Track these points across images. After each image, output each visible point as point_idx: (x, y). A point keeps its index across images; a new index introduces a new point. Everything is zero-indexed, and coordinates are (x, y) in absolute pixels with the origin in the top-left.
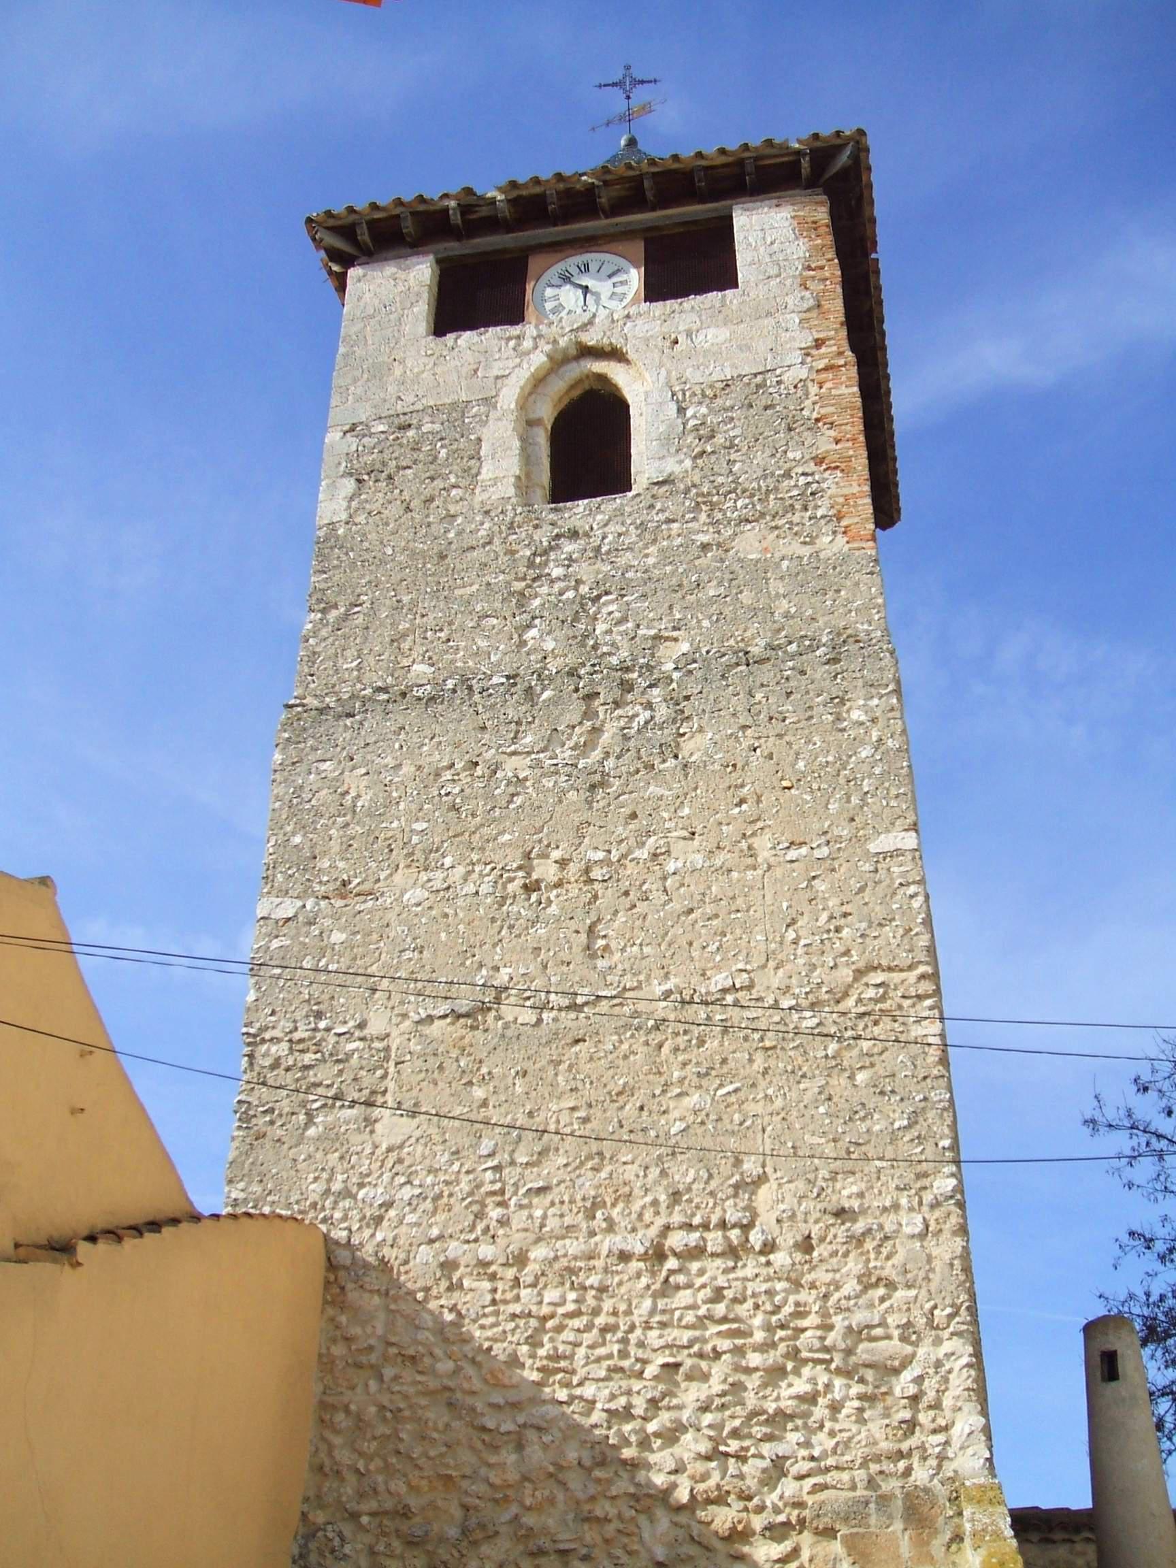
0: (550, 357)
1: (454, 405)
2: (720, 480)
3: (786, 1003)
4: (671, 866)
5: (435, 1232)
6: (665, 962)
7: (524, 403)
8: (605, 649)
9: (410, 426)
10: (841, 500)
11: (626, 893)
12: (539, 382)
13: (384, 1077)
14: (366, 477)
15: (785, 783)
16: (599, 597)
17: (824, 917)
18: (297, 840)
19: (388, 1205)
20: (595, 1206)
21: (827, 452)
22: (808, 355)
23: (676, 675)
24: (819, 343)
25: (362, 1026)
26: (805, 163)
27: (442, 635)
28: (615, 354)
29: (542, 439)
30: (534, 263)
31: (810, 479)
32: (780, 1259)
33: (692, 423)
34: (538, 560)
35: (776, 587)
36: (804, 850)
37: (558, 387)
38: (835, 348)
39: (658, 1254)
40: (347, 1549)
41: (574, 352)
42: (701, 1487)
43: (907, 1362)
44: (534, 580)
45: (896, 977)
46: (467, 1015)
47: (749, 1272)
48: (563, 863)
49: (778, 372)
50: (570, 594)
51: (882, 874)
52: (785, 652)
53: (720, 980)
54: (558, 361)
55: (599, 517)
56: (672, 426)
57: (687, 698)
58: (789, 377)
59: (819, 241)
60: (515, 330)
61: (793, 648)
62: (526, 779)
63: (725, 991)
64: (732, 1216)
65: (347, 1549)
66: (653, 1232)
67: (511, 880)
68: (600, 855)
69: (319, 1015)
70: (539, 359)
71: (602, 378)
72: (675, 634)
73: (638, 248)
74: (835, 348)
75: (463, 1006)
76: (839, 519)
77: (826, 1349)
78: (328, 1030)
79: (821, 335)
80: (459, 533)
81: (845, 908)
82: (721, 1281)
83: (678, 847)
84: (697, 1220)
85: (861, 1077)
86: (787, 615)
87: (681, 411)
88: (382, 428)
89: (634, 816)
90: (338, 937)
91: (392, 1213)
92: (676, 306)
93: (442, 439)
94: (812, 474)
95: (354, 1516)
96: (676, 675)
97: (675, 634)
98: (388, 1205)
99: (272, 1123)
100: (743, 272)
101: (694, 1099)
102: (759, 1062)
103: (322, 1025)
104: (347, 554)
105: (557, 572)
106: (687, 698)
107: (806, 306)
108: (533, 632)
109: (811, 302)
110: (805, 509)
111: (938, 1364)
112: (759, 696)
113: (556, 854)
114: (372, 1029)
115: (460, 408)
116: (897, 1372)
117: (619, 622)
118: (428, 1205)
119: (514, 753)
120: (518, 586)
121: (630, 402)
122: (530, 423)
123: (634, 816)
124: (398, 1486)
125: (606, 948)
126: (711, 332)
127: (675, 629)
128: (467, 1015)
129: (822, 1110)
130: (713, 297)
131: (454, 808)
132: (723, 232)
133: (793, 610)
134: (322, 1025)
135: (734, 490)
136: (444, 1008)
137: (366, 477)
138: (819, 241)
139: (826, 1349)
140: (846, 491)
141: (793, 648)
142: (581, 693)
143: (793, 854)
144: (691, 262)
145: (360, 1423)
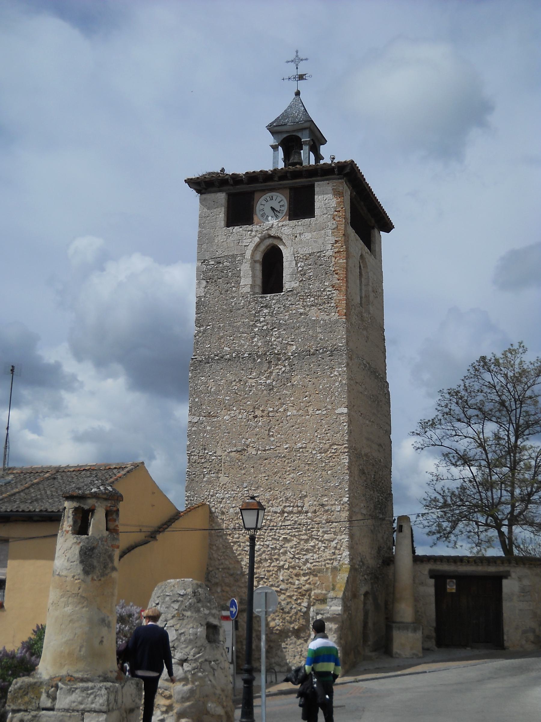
0: (260, 239)
1: (233, 255)
2: (306, 291)
3: (314, 452)
4: (289, 413)
5: (234, 505)
6: (287, 440)
7: (253, 255)
8: (274, 346)
10: (338, 301)
11: (278, 420)
12: (258, 246)
13: (221, 466)
15: (317, 392)
16: (273, 329)
17: (324, 430)
18: (197, 400)
19: (223, 499)
20: (270, 501)
22: (333, 246)
23: (292, 357)
24: (336, 242)
25: (215, 453)
28: (279, 238)
29: (259, 267)
30: (256, 195)
31: (330, 293)
32: (309, 514)
33: (300, 269)
35: (319, 330)
36: (320, 412)
37: (263, 247)
39: (283, 512)
40: (217, 576)
42: (290, 565)
43: (334, 539)
44: (256, 322)
45: (340, 447)
46: (240, 451)
47: (303, 517)
48: (263, 411)
50: (265, 328)
51: (338, 419)
53: (299, 445)
54: (262, 240)
55: (273, 301)
56: (294, 270)
57: (294, 365)
60: (250, 227)
62: (254, 386)
63: (300, 448)
64: (299, 504)
65: (217, 576)
66: (282, 507)
67: (250, 415)
68: (272, 409)
69: (205, 449)
70: (257, 240)
72: (292, 343)
73: (288, 192)
75: (239, 448)
76: (337, 308)
77: (318, 536)
78: (207, 453)
80: (235, 304)
81: (329, 428)
82: (296, 519)
83: (290, 408)
84: (292, 505)
85: (329, 472)
86: (321, 339)
87: (296, 264)
88: (213, 263)
89: (280, 399)
90: (208, 428)
91: (224, 500)
92: (297, 223)
94: (331, 291)
95: (218, 569)
96: (292, 357)
97: (292, 343)
98: (223, 499)
99: (195, 477)
100: (317, 212)
101: (291, 476)
102: (307, 467)
103: (206, 452)
105: (262, 319)
106: (294, 365)
108: (256, 339)
109: (335, 226)
110: (328, 303)
111: (341, 540)
112: (312, 365)
113: (261, 409)
114: (218, 453)
115: (234, 256)
116: (332, 541)
117: (278, 338)
118: (232, 499)
119: (250, 378)
122: (255, 262)
123: (280, 399)
124: (227, 562)
125: (272, 435)
126: (306, 234)
127: (292, 341)
128: (240, 451)
129: (320, 480)
130: (307, 220)
131: (236, 393)
132: (313, 186)
134: (206, 452)
135: (310, 295)
136: (235, 449)
139: (318, 536)
140: (340, 298)
142: (267, 361)
143: (318, 412)
144: (301, 207)
145: (218, 549)
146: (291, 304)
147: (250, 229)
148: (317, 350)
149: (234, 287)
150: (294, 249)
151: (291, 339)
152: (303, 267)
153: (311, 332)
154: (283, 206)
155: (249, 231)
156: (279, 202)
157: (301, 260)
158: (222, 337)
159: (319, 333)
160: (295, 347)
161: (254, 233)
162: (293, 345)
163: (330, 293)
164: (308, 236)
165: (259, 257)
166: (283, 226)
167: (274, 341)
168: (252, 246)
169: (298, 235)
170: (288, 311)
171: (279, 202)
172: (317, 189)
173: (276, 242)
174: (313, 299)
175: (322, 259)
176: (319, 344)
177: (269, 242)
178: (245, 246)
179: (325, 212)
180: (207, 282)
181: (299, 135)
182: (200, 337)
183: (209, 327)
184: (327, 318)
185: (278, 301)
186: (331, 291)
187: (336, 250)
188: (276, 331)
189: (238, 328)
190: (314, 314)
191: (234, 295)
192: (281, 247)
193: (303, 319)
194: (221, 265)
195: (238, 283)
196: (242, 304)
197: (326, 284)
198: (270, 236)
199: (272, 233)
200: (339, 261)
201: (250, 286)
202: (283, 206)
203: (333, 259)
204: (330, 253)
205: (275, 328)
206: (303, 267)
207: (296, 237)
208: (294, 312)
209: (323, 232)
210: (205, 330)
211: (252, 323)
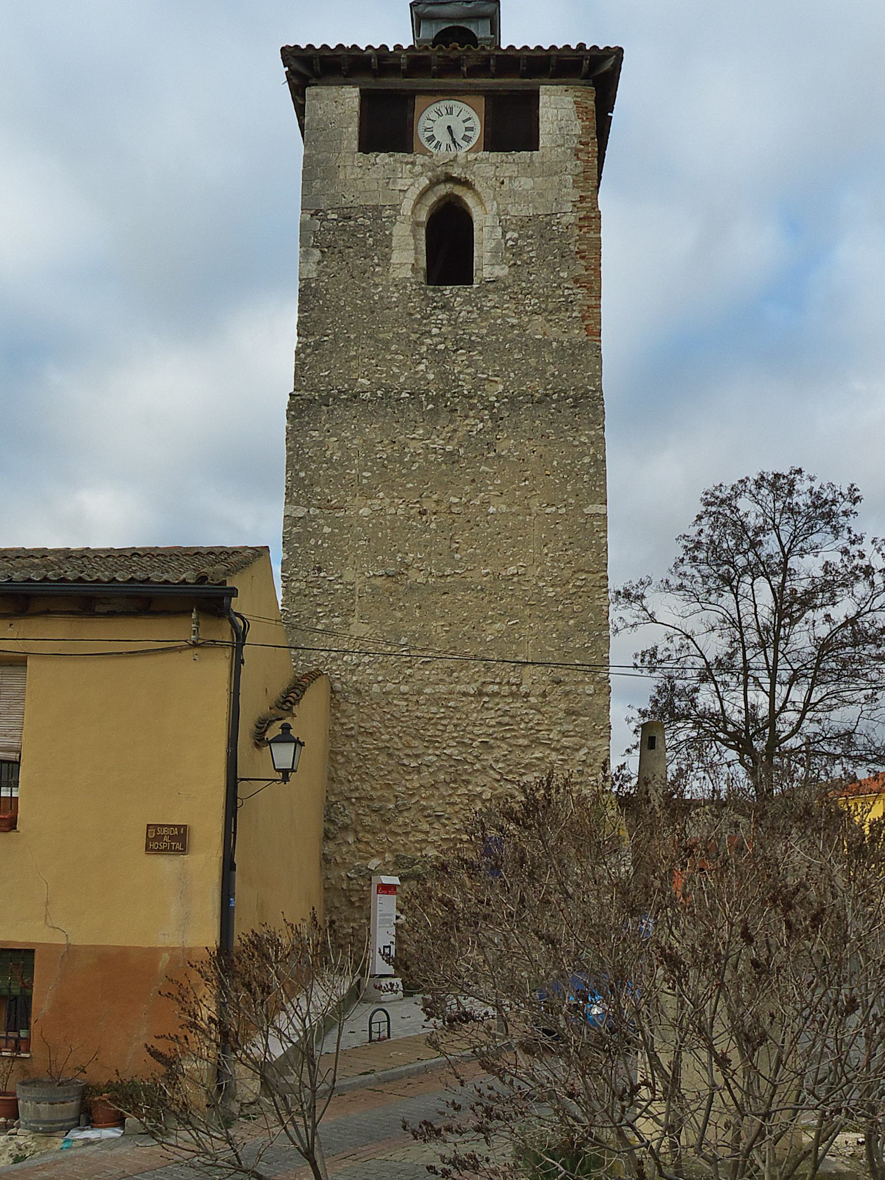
1: (375, 208)
2: (524, 284)
3: (541, 584)
4: (492, 510)
5: (380, 678)
6: (486, 558)
8: (460, 383)
9: (350, 217)
10: (586, 308)
11: (469, 521)
12: (423, 194)
13: (352, 603)
14: (326, 250)
15: (547, 472)
16: (457, 350)
17: (561, 544)
18: (302, 474)
19: (358, 665)
20: (453, 671)
21: (580, 275)
22: (575, 206)
23: (496, 405)
24: (582, 199)
25: (340, 577)
26: (586, 63)
27: (373, 361)
28: (466, 184)
30: (419, 101)
31: (571, 292)
32: (532, 700)
33: (510, 243)
34: (425, 321)
35: (548, 358)
36: (554, 509)
37: (432, 199)
38: (590, 205)
39: (480, 694)
40: (347, 812)
41: (443, 178)
42: (496, 792)
43: (582, 746)
44: (422, 334)
45: (591, 576)
46: (393, 576)
47: (519, 705)
48: (437, 502)
49: (559, 215)
50: (442, 347)
51: (588, 526)
52: (551, 398)
53: (512, 570)
54: (434, 183)
56: (499, 243)
57: (502, 419)
58: (564, 220)
59: (587, 123)
60: (409, 158)
61: (555, 396)
62: (420, 454)
63: (513, 575)
64: (513, 680)
65: (347, 812)
66: (478, 684)
67: (412, 508)
68: (457, 500)
69: (320, 570)
70: (424, 182)
71: (458, 198)
72: (496, 379)
73: (481, 101)
74: (590, 205)
75: (392, 570)
77: (549, 739)
78: (324, 577)
79: (583, 194)
80: (381, 298)
81: (570, 540)
82: (507, 708)
83: (494, 501)
84: (498, 680)
85: (571, 622)
86: (553, 375)
87: (504, 233)
88: (335, 216)
89: (473, 481)
90: (327, 530)
91: (360, 668)
92: (504, 158)
93: (370, 231)
95: (348, 799)
96: (496, 405)
97: (496, 379)
98: (358, 665)
99: (299, 622)
101: (497, 626)
102: (527, 612)
103: (322, 574)
104: (318, 301)
106: (502, 419)
107: (577, 172)
108: (422, 367)
109: (581, 169)
110: (567, 310)
111: (594, 748)
112: (538, 422)
113: (435, 497)
114: (345, 579)
115: (377, 209)
116: (577, 750)
118: (377, 665)
119: (414, 439)
120: (414, 337)
121: (475, 218)
122: (418, 224)
123: (473, 481)
124: (367, 786)
125: (457, 549)
128: (393, 576)
129: (554, 635)
131: (384, 466)
133: (557, 373)
134: (322, 574)
136: (381, 572)
137: (326, 250)
138: (587, 123)
139: (549, 739)
140: (588, 303)
141: (555, 396)
142: (447, 409)
143: (548, 510)
145: (349, 761)
146: (494, 307)
147: (410, 160)
148: (547, 395)
149: (378, 265)
150: (498, 204)
151: (494, 371)
152: (518, 239)
153: (533, 361)
154: (471, 129)
155: (407, 163)
156: (464, 122)
157: (512, 227)
158: (355, 357)
159: (549, 363)
160: (501, 388)
161: (418, 169)
162: (496, 382)
163: (571, 292)
164: (526, 183)
165: (423, 217)
166: (476, 159)
167: (459, 372)
168: (413, 194)
169: (506, 181)
170: (486, 320)
171: (464, 122)
172: (543, 99)
173: (458, 191)
174: (537, 301)
175: (554, 228)
176: (549, 384)
177: (443, 189)
178: (400, 191)
179: (560, 142)
180: (322, 252)
181: (472, 28)
182: (309, 355)
183: (326, 338)
184: (565, 338)
185: (468, 301)
186: (571, 289)
187: (583, 214)
188: (463, 354)
189: (387, 343)
190: (538, 327)
191: (377, 280)
192: (470, 200)
193: (518, 335)
194: (352, 223)
195: (386, 258)
196: (394, 299)
197: (562, 274)
198: (449, 179)
199: (456, 172)
200: (587, 235)
201: (410, 266)
202: (471, 129)
203: (577, 231)
204: (570, 218)
205: (461, 349)
206: (515, 240)
207: (503, 183)
208: (499, 321)
209: (556, 178)
210: (319, 344)
211: (414, 337)
